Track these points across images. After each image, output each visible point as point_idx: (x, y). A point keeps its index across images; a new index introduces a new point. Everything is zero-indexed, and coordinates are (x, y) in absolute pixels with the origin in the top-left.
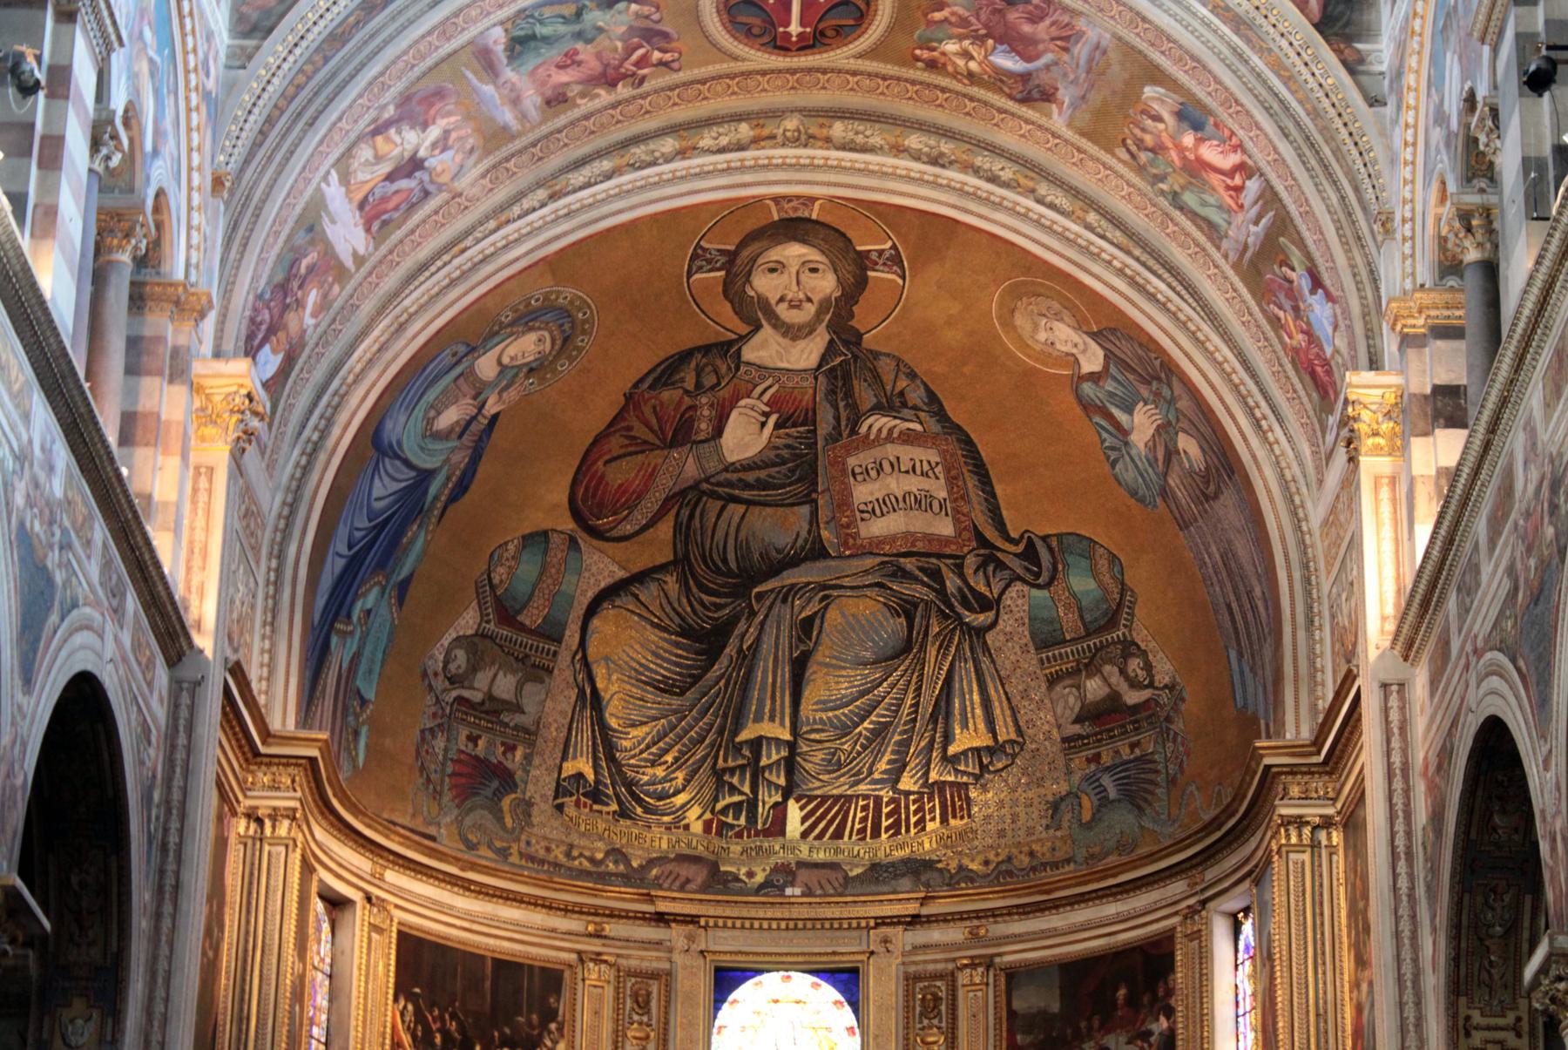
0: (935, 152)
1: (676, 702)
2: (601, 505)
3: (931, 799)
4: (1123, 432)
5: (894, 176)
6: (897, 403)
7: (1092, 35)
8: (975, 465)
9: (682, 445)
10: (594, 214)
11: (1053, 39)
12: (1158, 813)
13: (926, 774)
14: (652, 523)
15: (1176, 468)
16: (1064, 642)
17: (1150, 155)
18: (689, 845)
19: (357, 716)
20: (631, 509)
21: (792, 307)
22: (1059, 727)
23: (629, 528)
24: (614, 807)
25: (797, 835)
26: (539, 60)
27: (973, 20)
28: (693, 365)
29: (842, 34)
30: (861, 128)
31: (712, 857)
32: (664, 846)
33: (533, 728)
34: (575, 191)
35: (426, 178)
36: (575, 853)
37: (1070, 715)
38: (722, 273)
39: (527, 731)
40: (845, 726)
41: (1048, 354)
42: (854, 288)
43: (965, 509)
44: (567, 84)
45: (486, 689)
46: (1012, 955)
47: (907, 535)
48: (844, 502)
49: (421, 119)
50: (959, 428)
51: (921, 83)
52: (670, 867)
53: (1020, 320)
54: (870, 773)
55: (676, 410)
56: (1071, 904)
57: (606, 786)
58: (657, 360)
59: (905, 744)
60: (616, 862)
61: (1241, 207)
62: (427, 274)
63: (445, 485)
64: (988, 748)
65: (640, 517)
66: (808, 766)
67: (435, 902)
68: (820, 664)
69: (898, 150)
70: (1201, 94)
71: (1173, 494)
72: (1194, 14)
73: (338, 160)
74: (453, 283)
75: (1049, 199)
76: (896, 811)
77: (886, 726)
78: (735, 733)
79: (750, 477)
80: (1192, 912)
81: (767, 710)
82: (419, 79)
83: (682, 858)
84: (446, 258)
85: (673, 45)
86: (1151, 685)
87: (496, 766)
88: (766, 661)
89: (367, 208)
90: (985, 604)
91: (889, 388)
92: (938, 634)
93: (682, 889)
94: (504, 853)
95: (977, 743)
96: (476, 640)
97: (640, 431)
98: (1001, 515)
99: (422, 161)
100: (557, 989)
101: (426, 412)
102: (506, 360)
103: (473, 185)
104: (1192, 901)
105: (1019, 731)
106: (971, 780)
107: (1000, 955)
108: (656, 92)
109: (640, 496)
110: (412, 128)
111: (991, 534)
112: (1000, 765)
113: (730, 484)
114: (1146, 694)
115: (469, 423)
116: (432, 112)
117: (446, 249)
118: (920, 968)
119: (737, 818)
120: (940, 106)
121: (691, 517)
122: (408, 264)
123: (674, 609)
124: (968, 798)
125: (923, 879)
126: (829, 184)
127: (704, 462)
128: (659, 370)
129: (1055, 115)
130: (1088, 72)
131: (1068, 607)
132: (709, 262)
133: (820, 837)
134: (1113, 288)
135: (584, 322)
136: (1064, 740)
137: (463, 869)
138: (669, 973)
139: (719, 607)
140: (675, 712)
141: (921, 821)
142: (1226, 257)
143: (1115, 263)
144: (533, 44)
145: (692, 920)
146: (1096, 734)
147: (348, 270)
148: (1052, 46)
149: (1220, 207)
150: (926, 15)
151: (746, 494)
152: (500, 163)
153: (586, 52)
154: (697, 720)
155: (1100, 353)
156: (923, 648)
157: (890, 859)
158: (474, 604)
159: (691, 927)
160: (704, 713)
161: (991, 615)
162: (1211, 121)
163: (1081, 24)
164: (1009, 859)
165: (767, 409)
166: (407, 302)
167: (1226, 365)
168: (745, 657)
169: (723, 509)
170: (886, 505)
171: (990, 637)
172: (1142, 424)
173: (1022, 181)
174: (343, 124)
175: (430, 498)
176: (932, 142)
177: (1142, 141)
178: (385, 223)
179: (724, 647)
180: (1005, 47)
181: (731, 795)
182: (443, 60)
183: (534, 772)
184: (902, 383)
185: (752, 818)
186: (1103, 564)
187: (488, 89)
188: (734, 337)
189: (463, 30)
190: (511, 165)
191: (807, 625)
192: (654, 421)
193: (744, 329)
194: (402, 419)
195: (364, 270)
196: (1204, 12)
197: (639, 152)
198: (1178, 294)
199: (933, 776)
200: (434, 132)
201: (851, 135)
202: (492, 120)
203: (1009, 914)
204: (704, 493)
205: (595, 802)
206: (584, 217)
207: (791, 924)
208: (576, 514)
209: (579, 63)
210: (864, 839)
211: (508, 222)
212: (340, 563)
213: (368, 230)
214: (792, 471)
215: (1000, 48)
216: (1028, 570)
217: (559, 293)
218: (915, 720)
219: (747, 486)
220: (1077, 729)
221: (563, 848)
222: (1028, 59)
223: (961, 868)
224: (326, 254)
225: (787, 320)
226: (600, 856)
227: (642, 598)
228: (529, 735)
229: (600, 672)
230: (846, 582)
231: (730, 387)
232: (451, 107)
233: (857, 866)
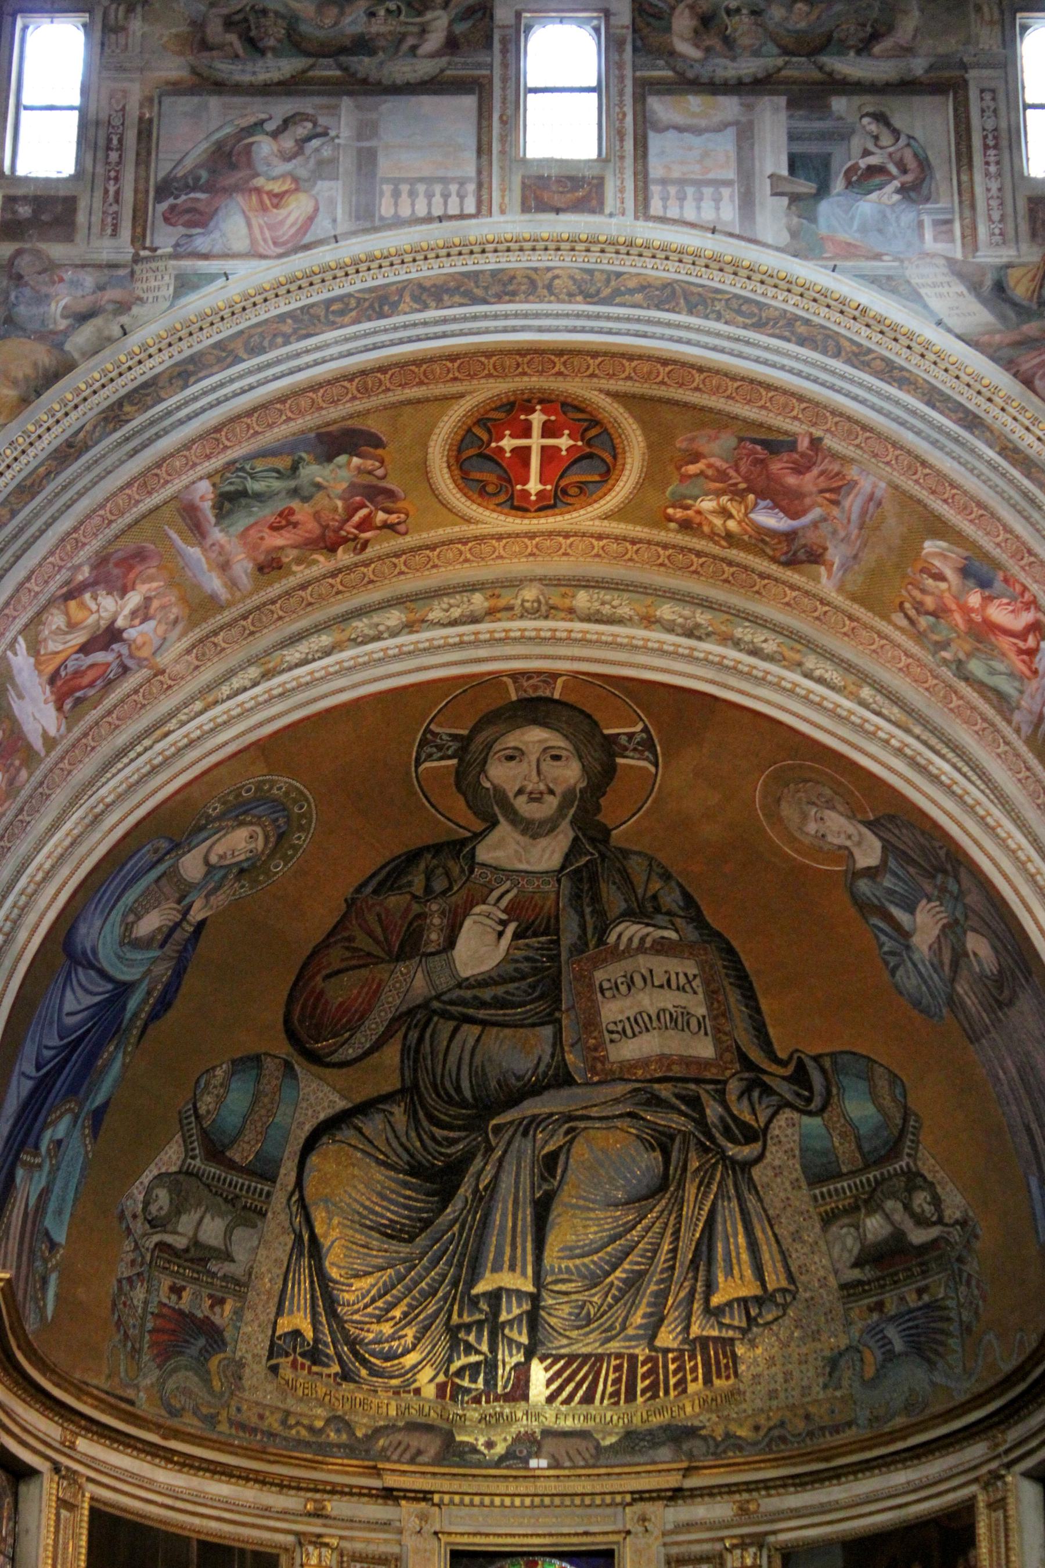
0: (690, 623)
1: (405, 1249)
3: (692, 1357)
4: (903, 934)
5: (646, 649)
6: (649, 907)
7: (866, 484)
8: (739, 978)
9: (411, 958)
11: (822, 491)
12: (950, 1367)
13: (687, 1329)
15: (965, 972)
16: (840, 1176)
17: (931, 619)
18: (421, 1410)
19: (45, 1261)
20: (354, 1030)
21: (531, 800)
22: (836, 1272)
23: (351, 1053)
25: (542, 1399)
26: (252, 520)
27: (732, 473)
28: (422, 866)
29: (585, 492)
30: (608, 598)
31: (446, 1426)
32: (393, 1412)
33: (244, 1279)
34: (290, 669)
35: (125, 651)
36: (292, 1421)
37: (848, 1258)
38: (455, 761)
39: (238, 1283)
40: (593, 1273)
41: (820, 848)
43: (727, 1029)
44: (281, 548)
45: (191, 1234)
46: (789, 1534)
47: (662, 1057)
48: (591, 1022)
49: (119, 584)
50: (719, 935)
51: (674, 547)
52: (399, 1437)
53: (787, 811)
54: (624, 1328)
55: (404, 917)
56: (855, 1473)
57: (326, 1344)
58: (381, 861)
59: (662, 1296)
60: (338, 1431)
61: (1035, 672)
62: (125, 760)
63: (145, 1001)
65: (364, 1040)
66: (553, 1321)
67: (133, 1475)
68: (565, 1205)
69: (649, 621)
70: (987, 544)
71: (962, 1003)
72: (980, 457)
73: (26, 626)
74: (155, 770)
75: (817, 673)
76: (652, 1372)
77: (641, 1274)
78: (472, 1283)
79: (487, 994)
81: (506, 1258)
82: (117, 537)
83: (413, 1427)
84: (147, 742)
85: (400, 505)
86: (940, 1221)
87: (202, 1321)
88: (505, 1202)
89: (59, 683)
90: (751, 1135)
91: (640, 891)
92: (698, 1169)
93: (412, 1461)
94: (211, 1420)
95: (743, 1293)
96: (181, 1177)
97: (363, 942)
98: (767, 1034)
99: (121, 631)
101: (125, 916)
102: (213, 859)
103: (176, 661)
104: (994, 1465)
105: (791, 1278)
106: (738, 1335)
107: (774, 1533)
108: (379, 558)
109: (362, 1018)
110: (109, 593)
111: (756, 1055)
112: (770, 1317)
113: (463, 1002)
114: (934, 1232)
115: (172, 930)
116: (132, 575)
117: (147, 732)
118: (683, 1549)
119: (473, 1380)
120: (695, 572)
121: (421, 1039)
122: (105, 750)
123: (402, 1145)
124: (734, 1355)
125: (685, 1447)
126: (573, 659)
127: (434, 977)
128: (384, 872)
129: (824, 580)
130: (861, 528)
131: (843, 1135)
132: (439, 748)
133: (568, 1401)
134: (891, 769)
135: (302, 816)
136: (843, 1287)
137: (165, 1437)
139: (453, 1142)
140: (404, 1261)
141: (682, 1383)
142: (1018, 731)
143: (893, 742)
144: (243, 501)
145: (425, 1496)
146: (878, 1279)
147: (37, 753)
148: (819, 499)
149: (1011, 675)
150: (679, 468)
151: (482, 1014)
152: (207, 637)
153: (302, 511)
154: (428, 1270)
155: (878, 844)
156: (681, 1186)
157: (647, 1426)
158: (178, 1137)
159: (423, 1504)
160: (435, 1263)
161: (757, 1147)
162: (1000, 575)
163: (853, 472)
164: (782, 1424)
165: (504, 917)
166: (103, 791)
167: (1020, 853)
168: (481, 1198)
169: (455, 1031)
170: (638, 1025)
171: (756, 1172)
173: (789, 654)
174: (31, 585)
175: (128, 1015)
176: (687, 612)
177: (921, 603)
178: (79, 701)
179: (458, 1187)
181: (467, 1353)
182: (144, 516)
184: (656, 885)
185: (491, 1381)
186: (882, 1084)
187: (194, 552)
189: (167, 482)
190: (219, 639)
191: (550, 1163)
192: (378, 930)
193: (479, 826)
194: (98, 923)
195: (55, 755)
196: (990, 454)
197: (361, 625)
198: (964, 775)
199: (695, 1330)
200: (134, 599)
201: (596, 605)
202: (197, 587)
203: (784, 1486)
204: (434, 1012)
205: (314, 1363)
207: (537, 1500)
208: (291, 1035)
209: (295, 525)
210: (617, 1403)
211: (216, 703)
212: (28, 1085)
213: (59, 708)
214: (533, 987)
215: (762, 504)
216: (798, 1095)
217: (272, 784)
218: (672, 1268)
219: (483, 1004)
220: (856, 1274)
221: (279, 1416)
222: (794, 516)
223: (728, 1435)
224: (12, 732)
225: (527, 815)
226: (319, 1424)
227: (367, 1131)
228: (239, 1286)
229: (319, 1216)
230: (594, 1112)
231: (464, 892)
232: (153, 571)
233: (610, 1434)
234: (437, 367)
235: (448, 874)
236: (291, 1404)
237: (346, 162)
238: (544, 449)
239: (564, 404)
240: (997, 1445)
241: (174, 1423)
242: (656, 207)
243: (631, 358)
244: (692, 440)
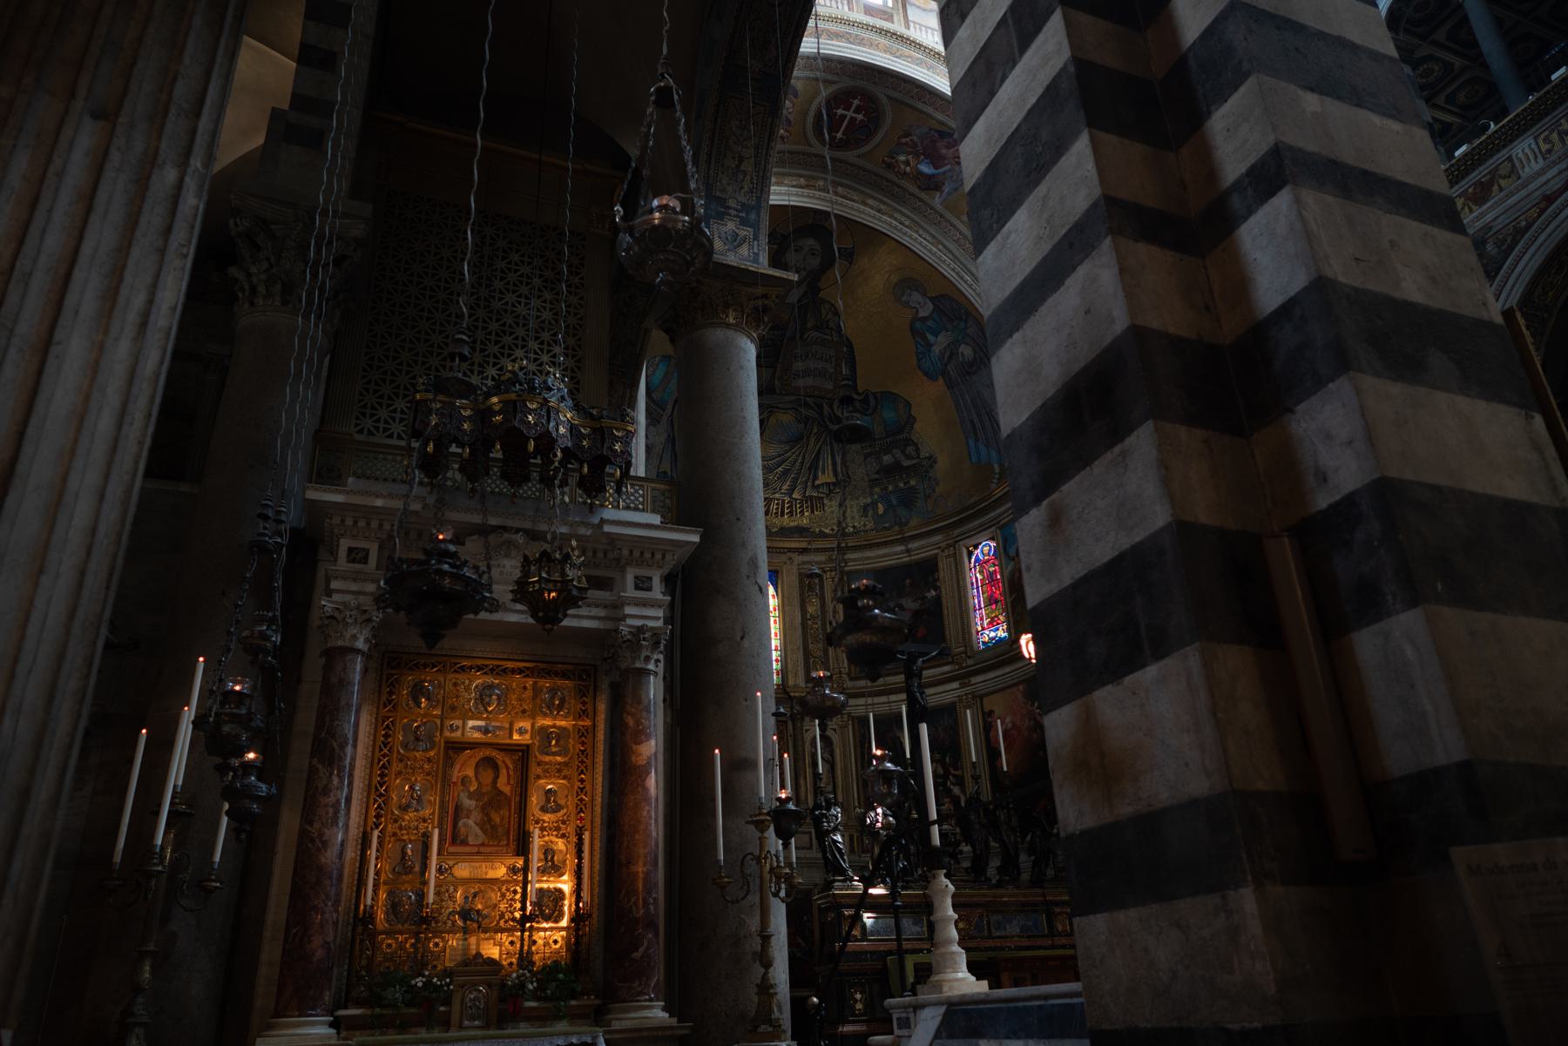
4: (929, 345)
22: (868, 475)
27: (919, 145)
64: (833, 483)
69: (865, 204)
80: (949, 546)
86: (918, 457)
91: (823, 316)
114: (914, 462)
141: (802, 512)
155: (931, 307)
156: (808, 439)
172: (940, 342)
180: (928, 161)
215: (925, 161)
222: (936, 168)
223: (820, 531)
230: (780, 406)
238: (852, 118)
240: (948, 535)
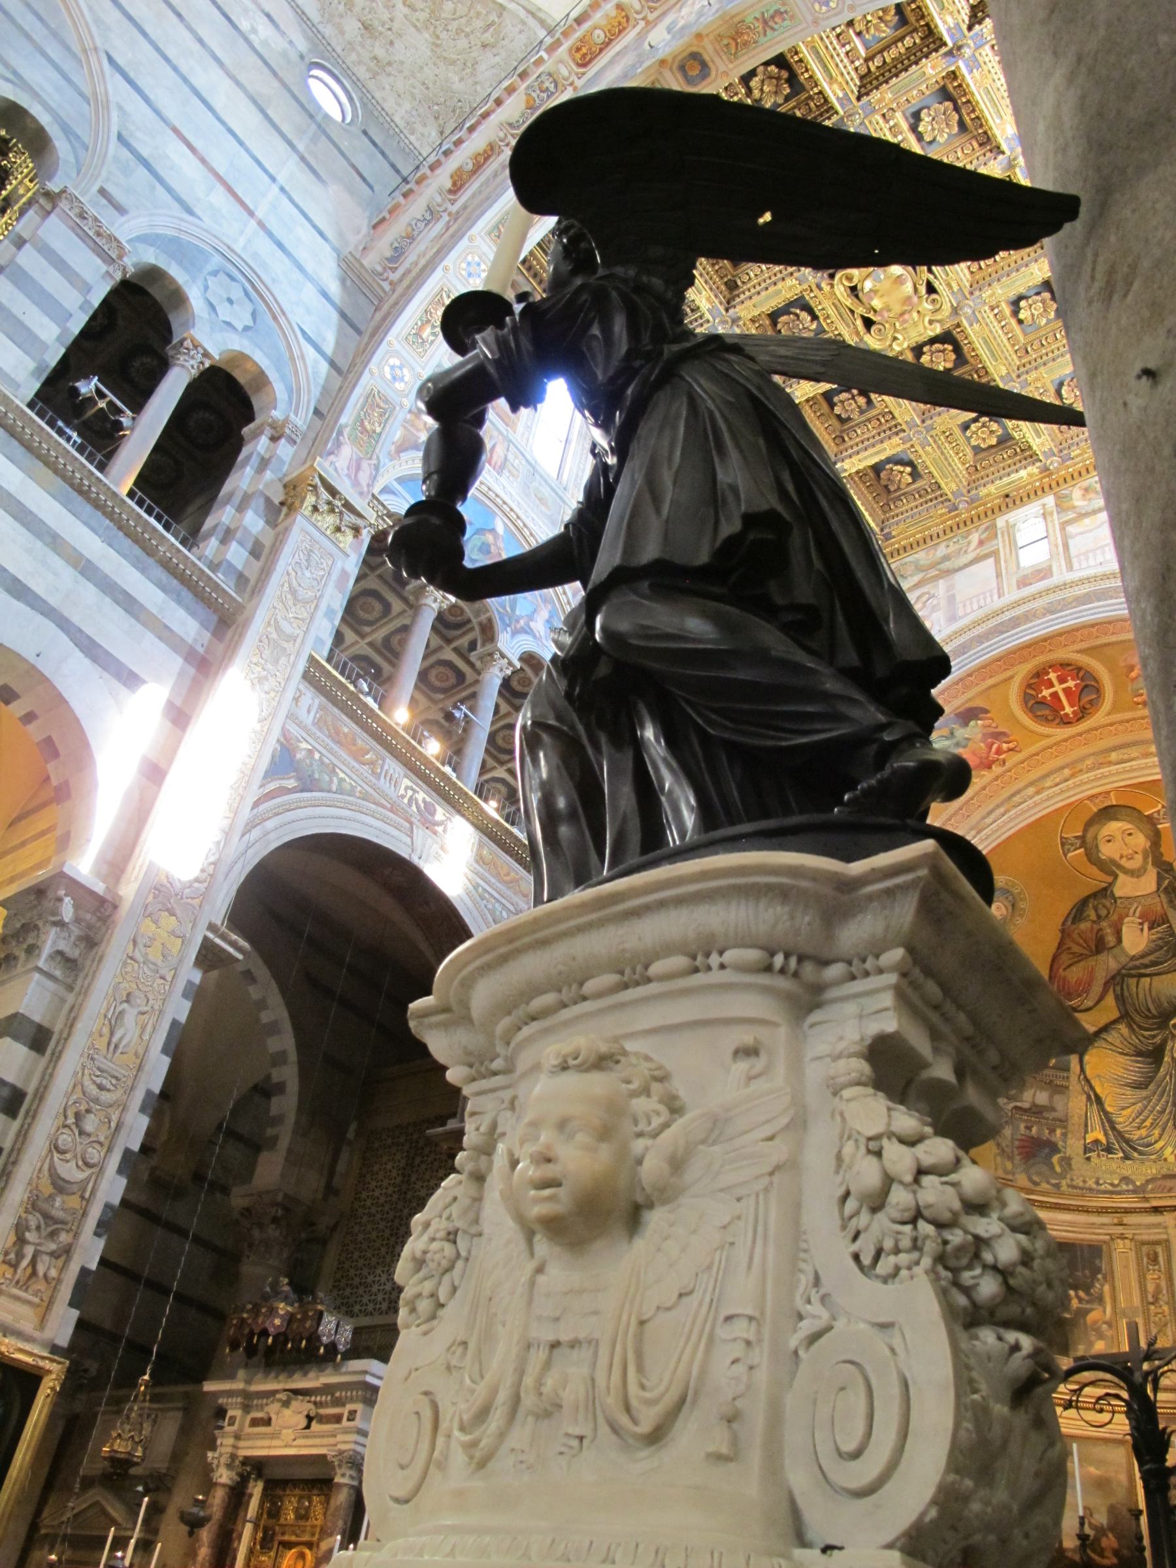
1: (1144, 1093)
2: (1069, 994)
10: (999, 833)
14: (1102, 998)
20: (1087, 992)
24: (1121, 1155)
29: (1095, 704)
39: (1061, 1121)
42: (1156, 838)
45: (1030, 1100)
52: (1159, 1183)
60: (1127, 1184)
79: (1146, 961)
94: (1057, 1186)
97: (1076, 949)
100: (1100, 1256)
113: (1136, 967)
121: (1122, 989)
132: (1072, 845)
135: (1019, 893)
138: (1167, 1241)
139: (1154, 1037)
151: (1148, 971)
154: (1159, 1101)
160: (1162, 1096)
179: (1163, 1058)
183: (1069, 1142)
188: (1104, 885)
193: (1110, 879)
197: (1017, 799)
204: (1124, 975)
206: (994, 836)
214: (1167, 951)
219: (1146, 966)
226: (1116, 1182)
234: (994, 666)
235: (1104, 906)
236: (1099, 1174)
237: (943, 603)
238: (1064, 690)
239: (1061, 665)
241: (1038, 1189)
242: (1076, 566)
243: (1077, 630)
244: (1125, 660)
